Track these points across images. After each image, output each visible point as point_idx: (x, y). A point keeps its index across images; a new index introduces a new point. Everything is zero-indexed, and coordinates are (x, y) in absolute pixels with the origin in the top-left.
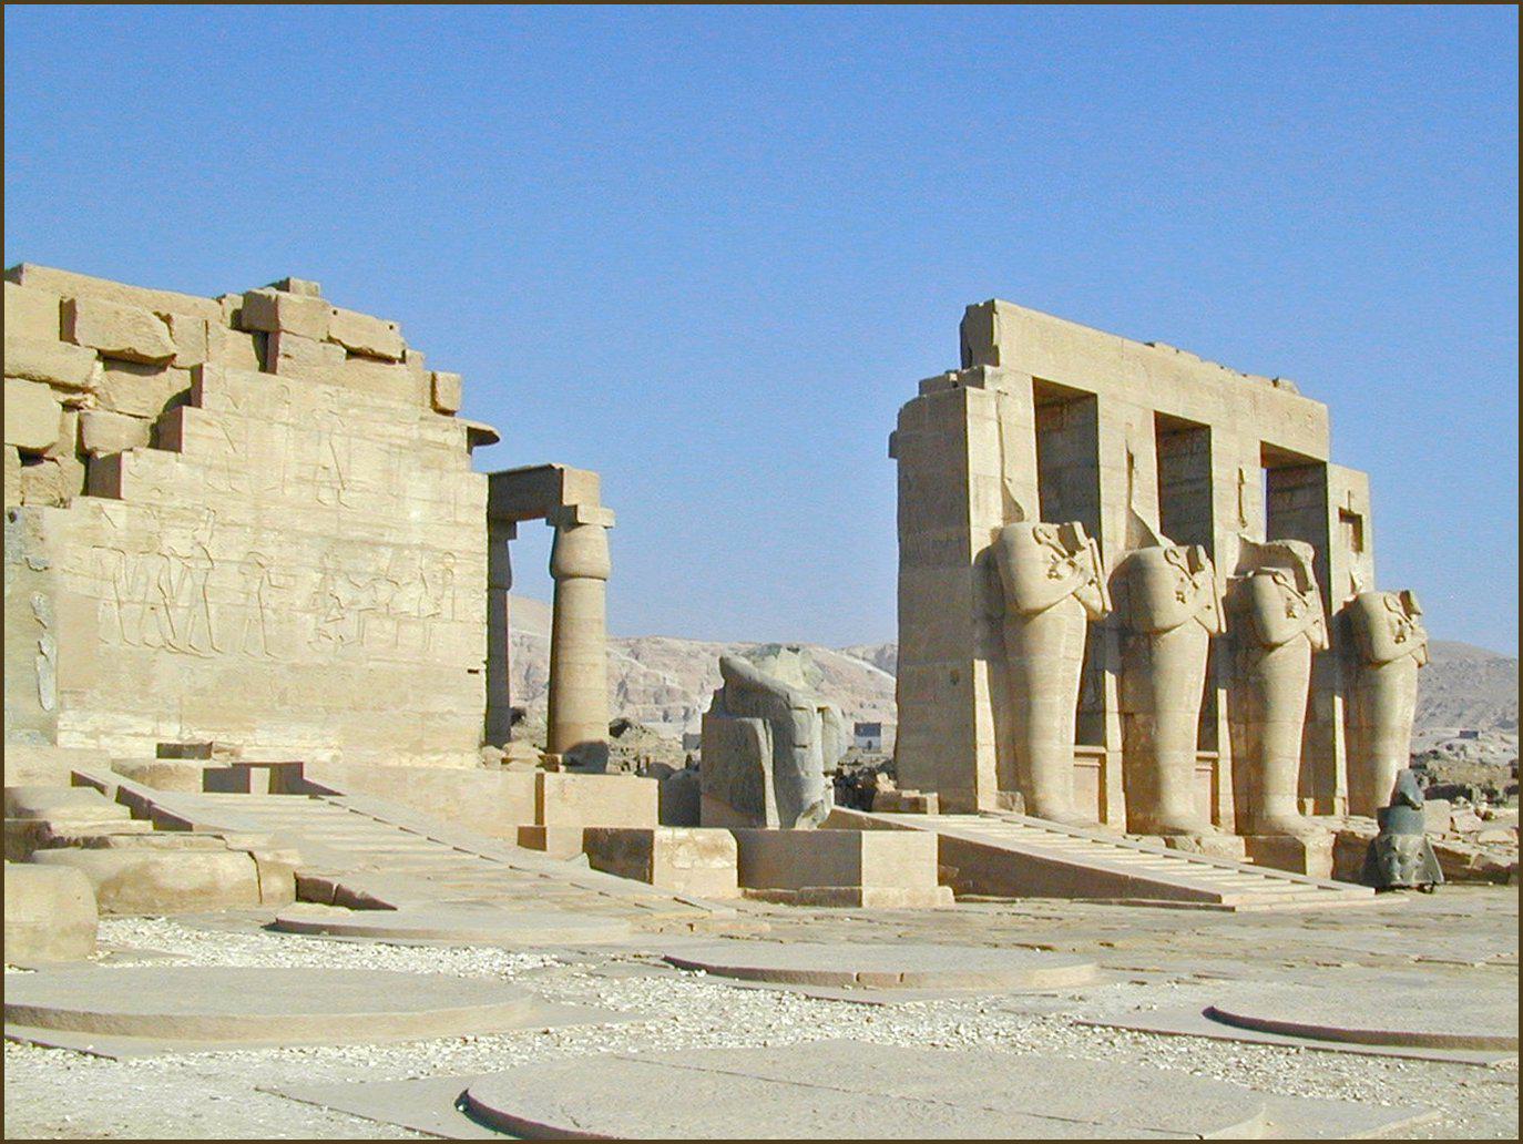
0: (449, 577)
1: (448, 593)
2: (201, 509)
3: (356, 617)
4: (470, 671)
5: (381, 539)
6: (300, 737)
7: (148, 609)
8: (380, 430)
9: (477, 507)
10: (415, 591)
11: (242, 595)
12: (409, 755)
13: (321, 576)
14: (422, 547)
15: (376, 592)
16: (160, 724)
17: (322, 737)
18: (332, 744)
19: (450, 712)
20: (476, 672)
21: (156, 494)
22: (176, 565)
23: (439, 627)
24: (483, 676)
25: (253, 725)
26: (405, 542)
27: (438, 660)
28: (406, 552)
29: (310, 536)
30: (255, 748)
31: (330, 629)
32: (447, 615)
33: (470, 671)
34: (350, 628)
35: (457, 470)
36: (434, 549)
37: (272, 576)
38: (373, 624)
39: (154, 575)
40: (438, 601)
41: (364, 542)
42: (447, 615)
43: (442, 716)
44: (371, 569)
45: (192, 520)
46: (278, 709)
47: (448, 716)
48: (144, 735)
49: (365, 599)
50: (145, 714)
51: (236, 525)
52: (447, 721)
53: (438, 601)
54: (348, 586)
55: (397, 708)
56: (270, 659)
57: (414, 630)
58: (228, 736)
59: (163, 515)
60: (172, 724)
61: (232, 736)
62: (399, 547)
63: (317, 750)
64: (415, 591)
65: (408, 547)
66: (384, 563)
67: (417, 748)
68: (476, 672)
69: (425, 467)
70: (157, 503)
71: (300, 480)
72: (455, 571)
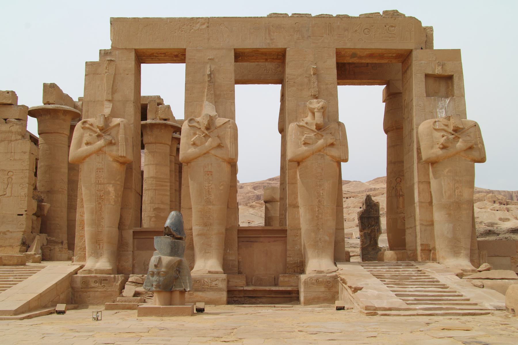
4: (19, 215)
9: (25, 153)
19: (8, 231)
20: (22, 215)
27: (4, 212)
32: (8, 194)
33: (19, 215)
35: (16, 140)
43: (4, 233)
47: (8, 233)
68: (22, 215)
72: (13, 177)
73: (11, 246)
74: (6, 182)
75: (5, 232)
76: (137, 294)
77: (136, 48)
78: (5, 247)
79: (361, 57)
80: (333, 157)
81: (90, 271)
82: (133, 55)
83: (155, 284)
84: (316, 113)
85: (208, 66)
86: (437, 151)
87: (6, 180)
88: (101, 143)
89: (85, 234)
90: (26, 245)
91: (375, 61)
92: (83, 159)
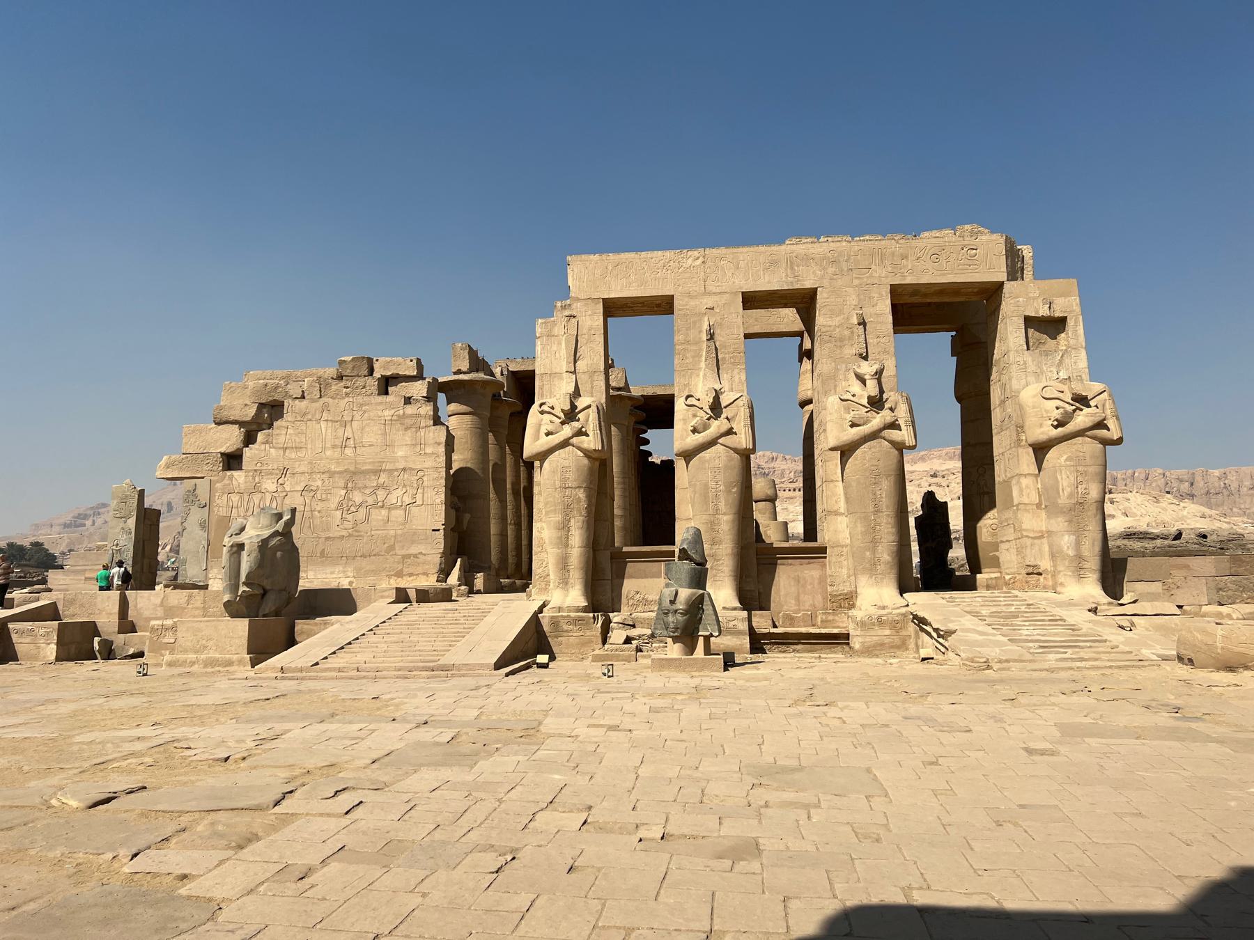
6: (332, 573)
8: (380, 413)
10: (399, 492)
23: (414, 510)
24: (442, 532)
29: (340, 473)
34: (361, 514)
36: (411, 469)
38: (374, 512)
39: (257, 502)
43: (416, 556)
49: (370, 500)
57: (398, 514)
62: (391, 471)
66: (381, 481)
67: (399, 574)
69: (407, 429)
71: (334, 447)
73: (426, 574)
76: (628, 640)
77: (606, 296)
79: (925, 295)
80: (892, 443)
81: (560, 609)
82: (600, 308)
83: (672, 626)
84: (868, 382)
85: (706, 319)
86: (1048, 431)
88: (567, 431)
89: (545, 557)
90: (445, 572)
91: (947, 300)
92: (543, 456)
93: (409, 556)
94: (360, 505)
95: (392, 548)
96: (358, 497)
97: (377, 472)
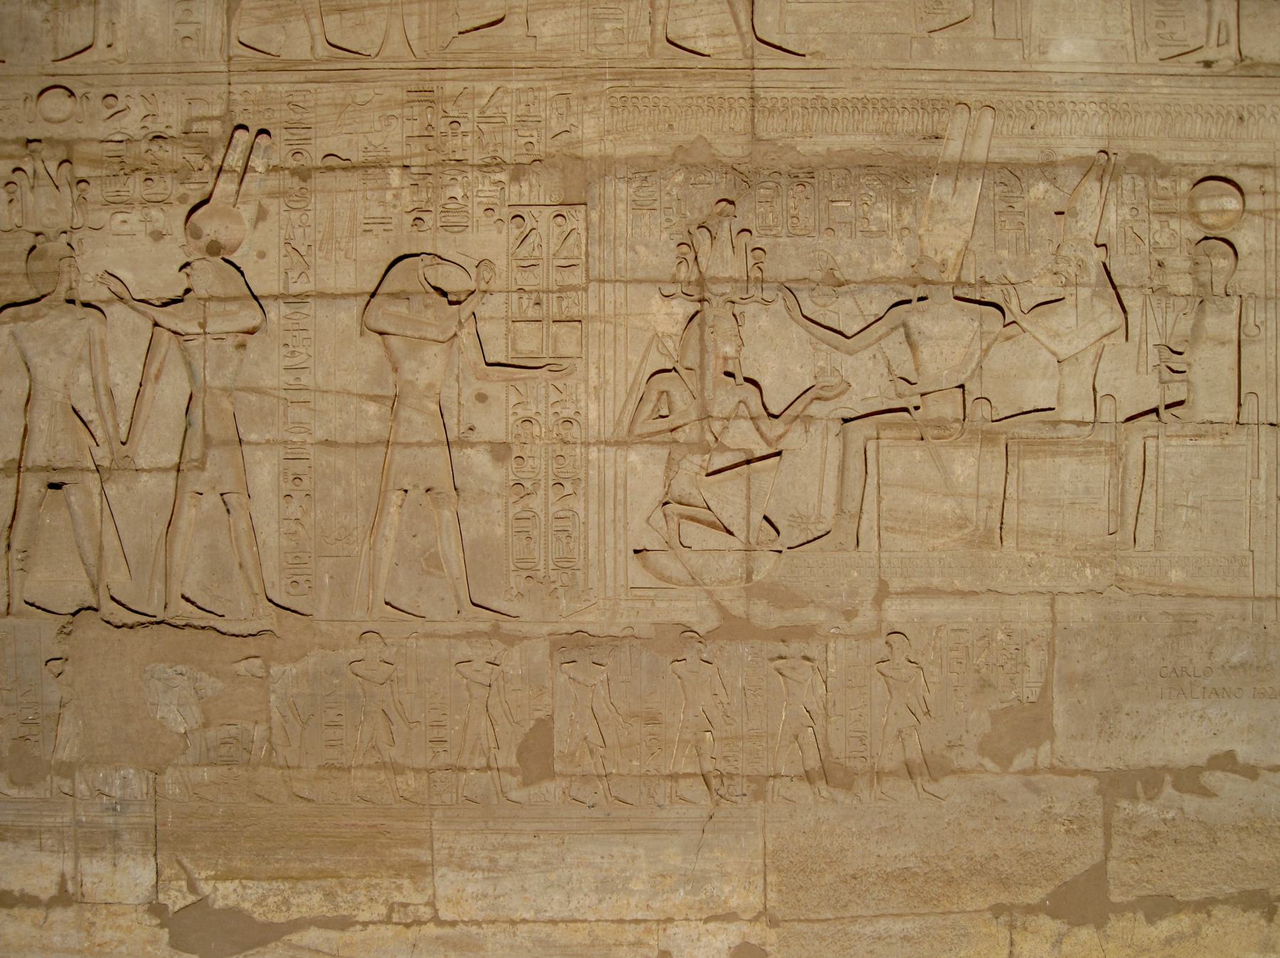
0: (1224, 263)
1: (1220, 323)
2: (215, 129)
3: (834, 446)
5: (926, 150)
6: (605, 886)
7: (33, 486)
11: (372, 408)
12: (1049, 925)
13: (681, 308)
14: (1103, 167)
15: (912, 346)
16: (84, 861)
17: (694, 881)
18: (734, 902)
19: (1225, 762)
21: (56, 104)
22: (127, 327)
23: (1176, 453)
25: (425, 856)
26: (1032, 155)
27: (1176, 575)
28: (1040, 189)
30: (431, 930)
31: (727, 499)
32: (1213, 402)
34: (807, 476)
37: (486, 329)
40: (1173, 361)
41: (869, 166)
42: (1213, 402)
43: (1189, 779)
44: (896, 265)
45: (183, 174)
46: (514, 795)
48: (30, 901)
49: (866, 381)
50: (30, 833)
51: (350, 168)
52: (1206, 793)
53: (1173, 361)
54: (797, 331)
55: (1004, 761)
56: (483, 622)
58: (330, 895)
59: (82, 172)
60: (125, 862)
61: (343, 896)
62: (1010, 173)
63: (671, 930)
64: (1080, 325)
65: (1047, 168)
70: (57, 131)
72: (1246, 239)
74: (1183, 285)
75: (1195, 770)
78: (1205, 906)
87: (1179, 261)
93: (1149, 780)
94: (793, 414)
95: (1031, 723)
96: (778, 354)
97: (901, 175)
